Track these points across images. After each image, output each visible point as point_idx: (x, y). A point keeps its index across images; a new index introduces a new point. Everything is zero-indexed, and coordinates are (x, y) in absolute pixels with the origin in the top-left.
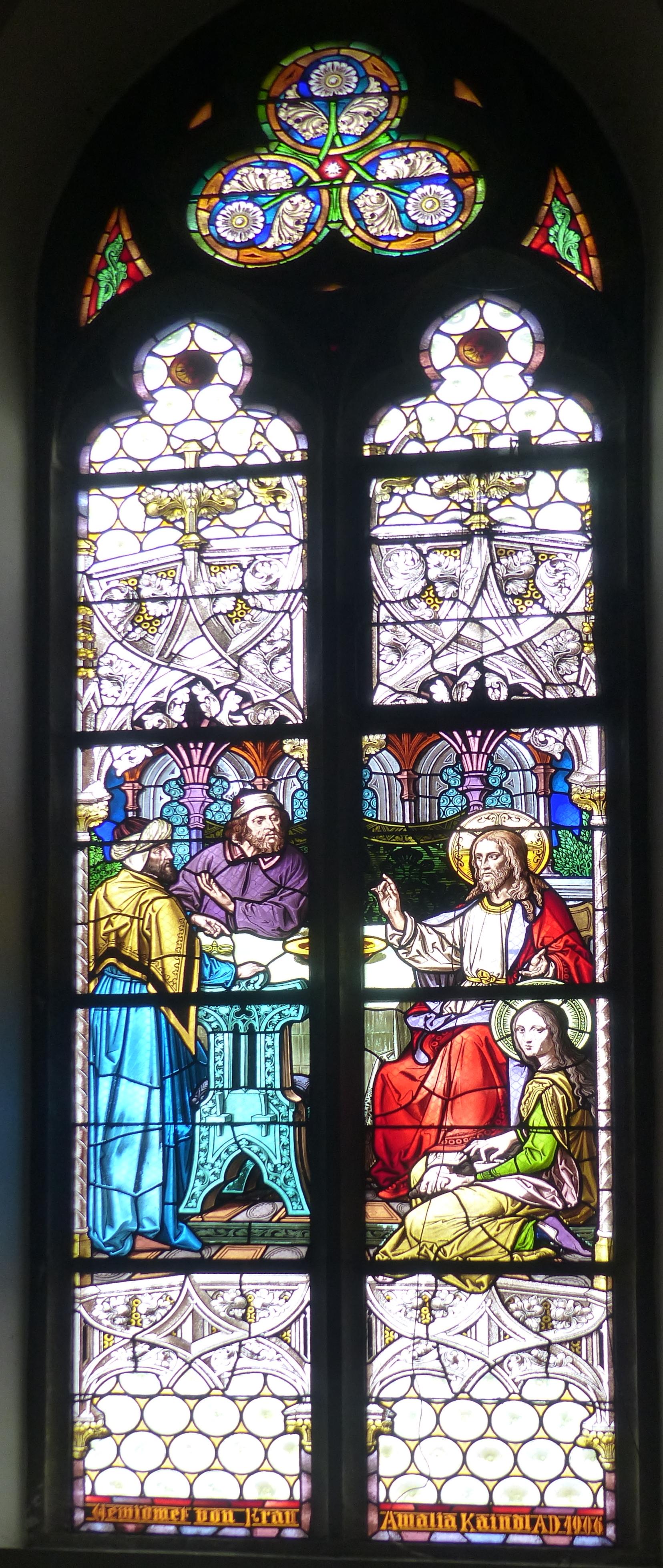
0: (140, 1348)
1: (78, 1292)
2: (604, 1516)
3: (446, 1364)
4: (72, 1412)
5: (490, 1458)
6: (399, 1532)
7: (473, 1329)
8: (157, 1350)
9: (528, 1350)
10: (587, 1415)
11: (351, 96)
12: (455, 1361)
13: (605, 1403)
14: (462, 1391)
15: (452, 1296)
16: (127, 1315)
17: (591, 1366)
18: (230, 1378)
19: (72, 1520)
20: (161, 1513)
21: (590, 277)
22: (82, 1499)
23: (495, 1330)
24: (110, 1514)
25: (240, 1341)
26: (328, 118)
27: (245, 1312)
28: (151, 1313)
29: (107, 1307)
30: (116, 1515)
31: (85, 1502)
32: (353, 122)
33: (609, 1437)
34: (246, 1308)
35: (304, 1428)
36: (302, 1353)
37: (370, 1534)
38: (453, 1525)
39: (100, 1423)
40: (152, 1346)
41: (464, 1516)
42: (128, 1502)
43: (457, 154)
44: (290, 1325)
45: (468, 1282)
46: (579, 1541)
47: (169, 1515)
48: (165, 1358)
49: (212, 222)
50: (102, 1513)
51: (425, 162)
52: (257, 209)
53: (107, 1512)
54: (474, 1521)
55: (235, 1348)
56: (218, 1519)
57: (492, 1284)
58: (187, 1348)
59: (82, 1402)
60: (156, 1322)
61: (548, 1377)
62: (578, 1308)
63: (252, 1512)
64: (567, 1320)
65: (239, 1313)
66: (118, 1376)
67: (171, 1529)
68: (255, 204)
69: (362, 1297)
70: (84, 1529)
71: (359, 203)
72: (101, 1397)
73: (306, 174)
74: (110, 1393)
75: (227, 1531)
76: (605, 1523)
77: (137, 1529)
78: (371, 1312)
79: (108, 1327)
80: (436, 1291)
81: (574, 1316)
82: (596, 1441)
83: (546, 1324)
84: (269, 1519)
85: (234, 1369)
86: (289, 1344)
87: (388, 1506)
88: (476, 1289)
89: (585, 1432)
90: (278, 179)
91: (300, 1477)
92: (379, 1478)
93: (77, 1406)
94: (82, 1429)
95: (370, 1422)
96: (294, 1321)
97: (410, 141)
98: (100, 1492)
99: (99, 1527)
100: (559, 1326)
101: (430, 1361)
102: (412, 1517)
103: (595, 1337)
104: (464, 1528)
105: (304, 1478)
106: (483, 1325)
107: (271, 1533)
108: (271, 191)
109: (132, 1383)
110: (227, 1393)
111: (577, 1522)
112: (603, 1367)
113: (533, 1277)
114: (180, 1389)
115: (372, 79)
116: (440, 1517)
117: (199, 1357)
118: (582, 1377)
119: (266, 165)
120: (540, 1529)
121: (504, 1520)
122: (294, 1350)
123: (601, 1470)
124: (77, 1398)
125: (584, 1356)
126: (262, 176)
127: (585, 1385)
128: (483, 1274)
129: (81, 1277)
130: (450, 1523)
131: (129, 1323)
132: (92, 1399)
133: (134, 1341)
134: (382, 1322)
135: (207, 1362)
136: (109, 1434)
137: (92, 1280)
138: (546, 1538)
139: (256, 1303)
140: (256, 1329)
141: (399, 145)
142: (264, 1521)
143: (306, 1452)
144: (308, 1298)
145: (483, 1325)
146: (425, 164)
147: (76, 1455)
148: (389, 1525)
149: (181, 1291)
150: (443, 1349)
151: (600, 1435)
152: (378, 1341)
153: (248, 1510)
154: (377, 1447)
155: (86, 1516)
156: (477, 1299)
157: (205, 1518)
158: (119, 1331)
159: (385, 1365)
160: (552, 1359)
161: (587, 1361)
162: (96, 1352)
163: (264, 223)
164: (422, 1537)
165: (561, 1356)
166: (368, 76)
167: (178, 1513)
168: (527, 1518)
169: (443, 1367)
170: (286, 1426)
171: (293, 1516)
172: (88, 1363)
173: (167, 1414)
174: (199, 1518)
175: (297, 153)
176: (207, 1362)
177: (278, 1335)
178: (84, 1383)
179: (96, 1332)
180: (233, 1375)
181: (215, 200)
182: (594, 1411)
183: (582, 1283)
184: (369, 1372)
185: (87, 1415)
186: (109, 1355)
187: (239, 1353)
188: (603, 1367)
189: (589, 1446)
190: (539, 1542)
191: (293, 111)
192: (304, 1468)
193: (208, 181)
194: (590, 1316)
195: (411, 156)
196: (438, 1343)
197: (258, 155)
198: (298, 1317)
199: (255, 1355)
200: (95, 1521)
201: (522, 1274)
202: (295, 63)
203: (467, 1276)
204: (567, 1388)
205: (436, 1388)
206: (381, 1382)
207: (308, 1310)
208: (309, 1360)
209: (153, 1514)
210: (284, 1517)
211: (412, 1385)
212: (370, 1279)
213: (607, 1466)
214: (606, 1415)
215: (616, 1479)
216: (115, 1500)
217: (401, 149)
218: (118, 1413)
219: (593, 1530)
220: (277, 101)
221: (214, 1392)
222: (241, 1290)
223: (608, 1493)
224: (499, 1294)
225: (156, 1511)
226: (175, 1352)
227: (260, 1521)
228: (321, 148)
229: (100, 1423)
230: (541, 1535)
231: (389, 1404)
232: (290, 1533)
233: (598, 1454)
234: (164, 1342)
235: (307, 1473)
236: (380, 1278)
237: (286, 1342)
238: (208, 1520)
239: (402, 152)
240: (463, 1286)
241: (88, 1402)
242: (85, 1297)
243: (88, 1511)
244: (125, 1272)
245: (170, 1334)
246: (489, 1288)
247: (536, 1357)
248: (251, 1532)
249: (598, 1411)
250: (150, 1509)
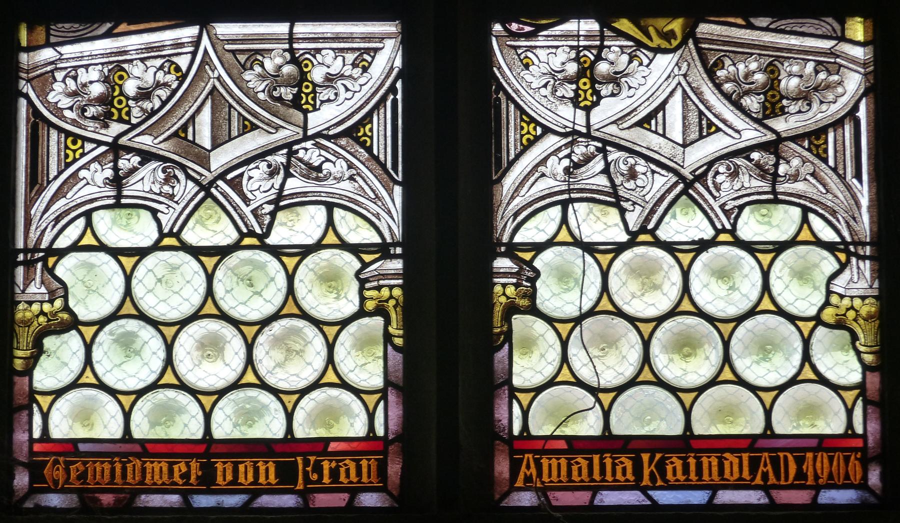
0: (124, 164)
1: (24, 57)
2: (864, 449)
3: (618, 180)
4: (13, 283)
5: (686, 350)
6: (543, 491)
7: (660, 115)
8: (154, 165)
9: (744, 152)
10: (837, 266)
12: (632, 175)
13: (864, 244)
14: (643, 230)
15: (625, 58)
16: (105, 100)
17: (842, 178)
18: (273, 214)
19: (10, 489)
20: (157, 469)
22: (25, 449)
23: (693, 117)
24: (73, 475)
25: (289, 146)
27: (299, 93)
28: (144, 94)
29: (72, 85)
30: (83, 476)
31: (32, 453)
33: (868, 308)
34: (299, 85)
35: (392, 302)
36: (389, 165)
37: (497, 497)
38: (630, 476)
39: (58, 303)
40: (147, 156)
41: (645, 457)
42: (103, 451)
44: (370, 115)
45: (651, 30)
46: (828, 497)
47: (171, 472)
48: (167, 181)
50: (60, 474)
53: (67, 471)
54: (661, 467)
55: (280, 158)
56: (250, 478)
57: (689, 33)
58: (204, 161)
59: (29, 265)
60: (154, 112)
61: (776, 201)
62: (822, 76)
63: (306, 463)
64: (804, 96)
65: (287, 93)
66: (88, 215)
67: (174, 499)
69: (485, 60)
70: (29, 504)
72: (62, 253)
74: (76, 247)
75: (265, 501)
76: (865, 463)
77: (118, 501)
78: (500, 87)
79: (74, 122)
80: (601, 48)
81: (816, 89)
82: (851, 314)
83: (773, 105)
84: (335, 473)
85: (280, 196)
86: (369, 150)
87: (526, 444)
88: (664, 45)
89: (834, 299)
91: (384, 397)
92: (513, 391)
93: (20, 271)
94: (28, 315)
95: (498, 289)
96: (376, 107)
98: (57, 432)
99: (54, 500)
100: (793, 108)
101: (593, 176)
102: (563, 462)
103: (848, 129)
104: (646, 481)
105: (392, 397)
106: (675, 108)
107: (339, 500)
109: (112, 228)
110: (270, 241)
111: (822, 464)
112: (860, 181)
113: (753, 20)
114: (191, 236)
116: (608, 462)
117: (222, 176)
118: (828, 200)
120: (765, 476)
121: (710, 462)
122: (376, 159)
123: (857, 366)
124: (21, 257)
125: (831, 162)
127: (834, 213)
128: (675, 16)
129: (30, 30)
130: (624, 470)
131: (108, 115)
132: (44, 260)
133: (116, 149)
134: (518, 106)
135: (236, 185)
136: (74, 323)
137: (48, 35)
138: (774, 493)
139: (317, 75)
140: (318, 120)
142: (326, 480)
143: (396, 348)
144: (398, 63)
145: (675, 108)
147: (18, 364)
148: (528, 479)
149: (194, 54)
150: (614, 155)
151: (857, 302)
152: (512, 139)
153: (299, 460)
154: (508, 335)
155: (31, 482)
156: (664, 61)
157: (229, 477)
158: (91, 130)
159: (522, 184)
160: (782, 169)
161: (835, 170)
162: (53, 172)
164: (581, 498)
165: (796, 162)
167: (184, 469)
168: (745, 456)
169: (613, 185)
170: (363, 299)
171: (374, 468)
172: (39, 193)
173: (171, 285)
174: (220, 480)
176: (236, 185)
177: (350, 133)
178: (33, 228)
179: (54, 134)
180: (278, 208)
182: (848, 261)
183: (825, 29)
184: (497, 198)
185: (36, 289)
186: (75, 174)
187: (287, 167)
188: (860, 181)
189: (839, 325)
190: (765, 501)
192: (392, 379)
194: (840, 90)
196: (606, 143)
198: (383, 99)
199: (313, 171)
200: (48, 490)
201: (736, 16)
203: (651, 21)
204: (805, 220)
205: (600, 225)
206: (516, 215)
207: (399, 85)
208: (400, 178)
209: (144, 470)
210: (359, 473)
211: (564, 220)
212: (498, 27)
213: (869, 358)
214: (866, 267)
215: (882, 382)
216: (82, 447)
218: (92, 286)
219: (847, 477)
221: (247, 241)
222: (291, 51)
223: (870, 409)
224: (699, 51)
225: (148, 465)
226: (183, 168)
227: (321, 476)
229: (58, 303)
230: (766, 488)
231: (527, 256)
232: (369, 500)
233: (854, 337)
234: (165, 149)
235: (395, 386)
236: (514, 27)
237: (363, 145)
238: (235, 481)
240: (645, 40)
241: (39, 265)
242: (36, 68)
243: (36, 469)
244: (103, 22)
245: (175, 134)
246: (684, 42)
247: (758, 165)
248: (306, 501)
249: (854, 260)
250: (138, 463)
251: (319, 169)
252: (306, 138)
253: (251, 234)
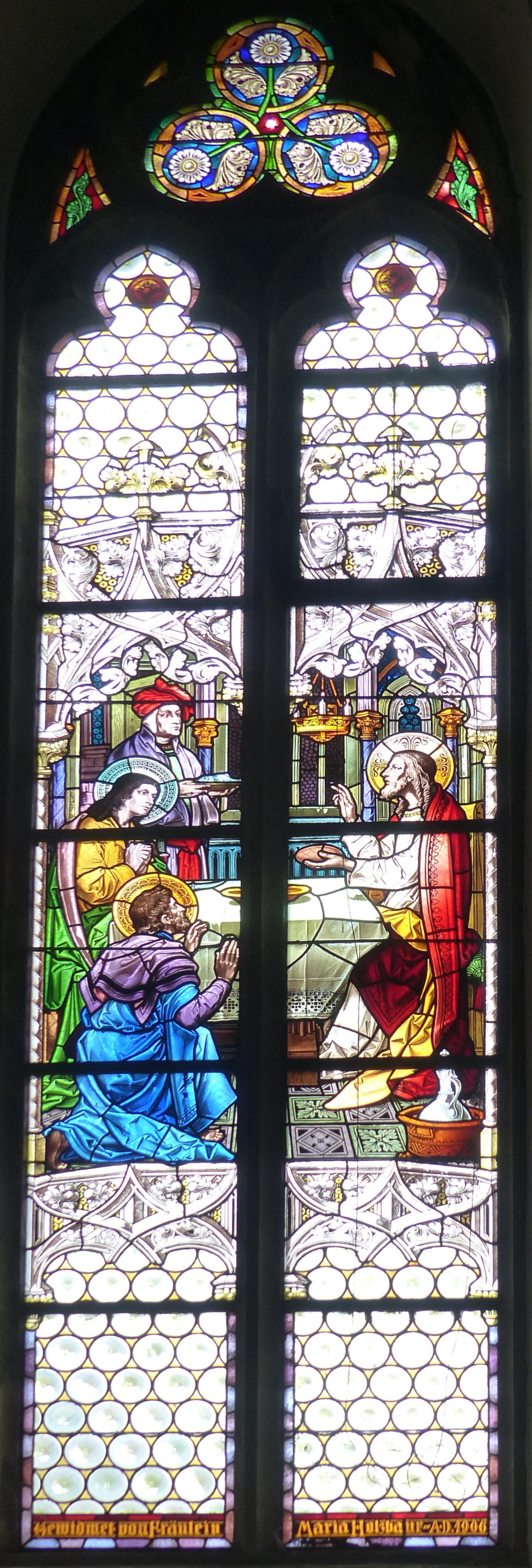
11: (286, 64)
26: (267, 82)
32: (287, 84)
43: (375, 117)
49: (166, 165)
51: (347, 122)
52: (204, 155)
68: (203, 151)
71: (291, 154)
73: (246, 128)
90: (223, 131)
97: (335, 105)
108: (217, 141)
115: (304, 51)
119: (212, 118)
126: (209, 127)
141: (327, 108)
146: (347, 124)
163: (210, 168)
166: (300, 47)
175: (239, 110)
181: (168, 147)
191: (236, 73)
193: (163, 130)
197: (206, 110)
202: (237, 33)
217: (327, 111)
220: (223, 66)
228: (260, 106)
239: (329, 114)
251: (192, 1231)
252: (185, 1217)
253: (155, 1263)
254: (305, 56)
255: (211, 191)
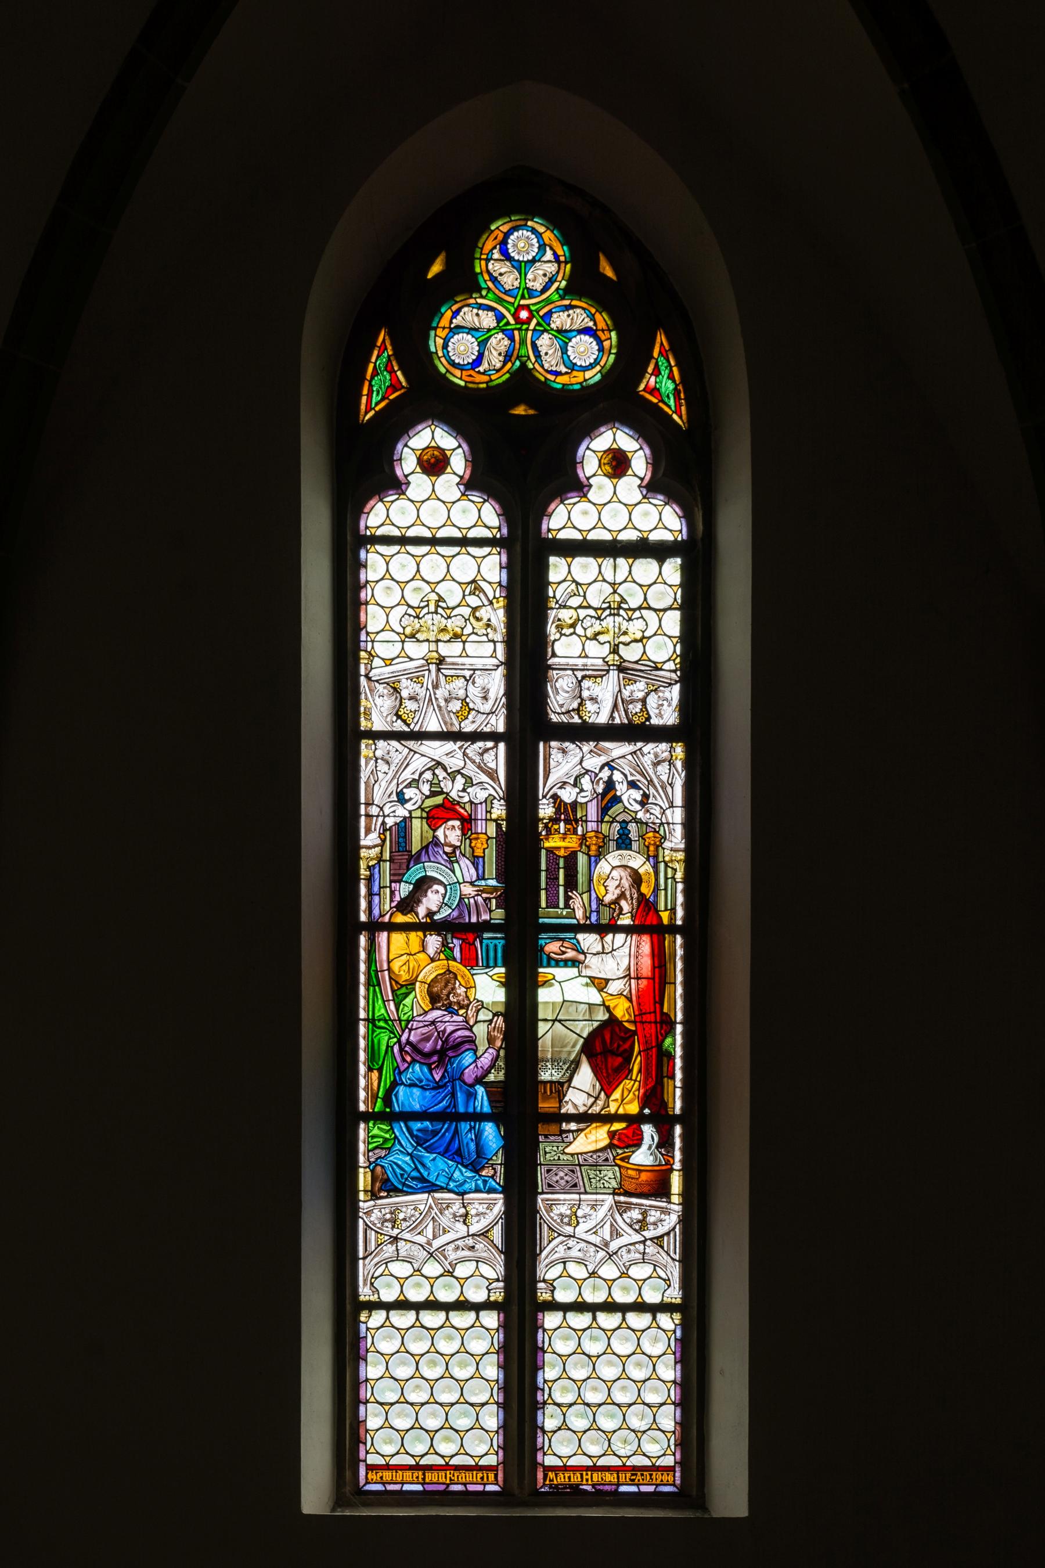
11: (533, 261)
21: (680, 417)
26: (520, 274)
49: (445, 346)
51: (579, 318)
52: (474, 340)
71: (538, 343)
115: (548, 249)
126: (477, 315)
141: (567, 302)
166: (545, 245)
191: (497, 266)
195: (571, 312)
228: (515, 298)
239: (568, 308)
254: (549, 255)
255: (479, 372)
